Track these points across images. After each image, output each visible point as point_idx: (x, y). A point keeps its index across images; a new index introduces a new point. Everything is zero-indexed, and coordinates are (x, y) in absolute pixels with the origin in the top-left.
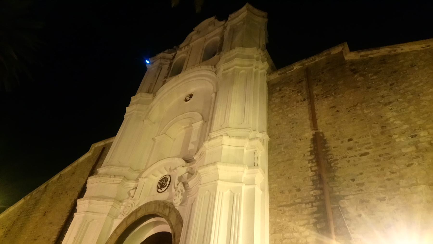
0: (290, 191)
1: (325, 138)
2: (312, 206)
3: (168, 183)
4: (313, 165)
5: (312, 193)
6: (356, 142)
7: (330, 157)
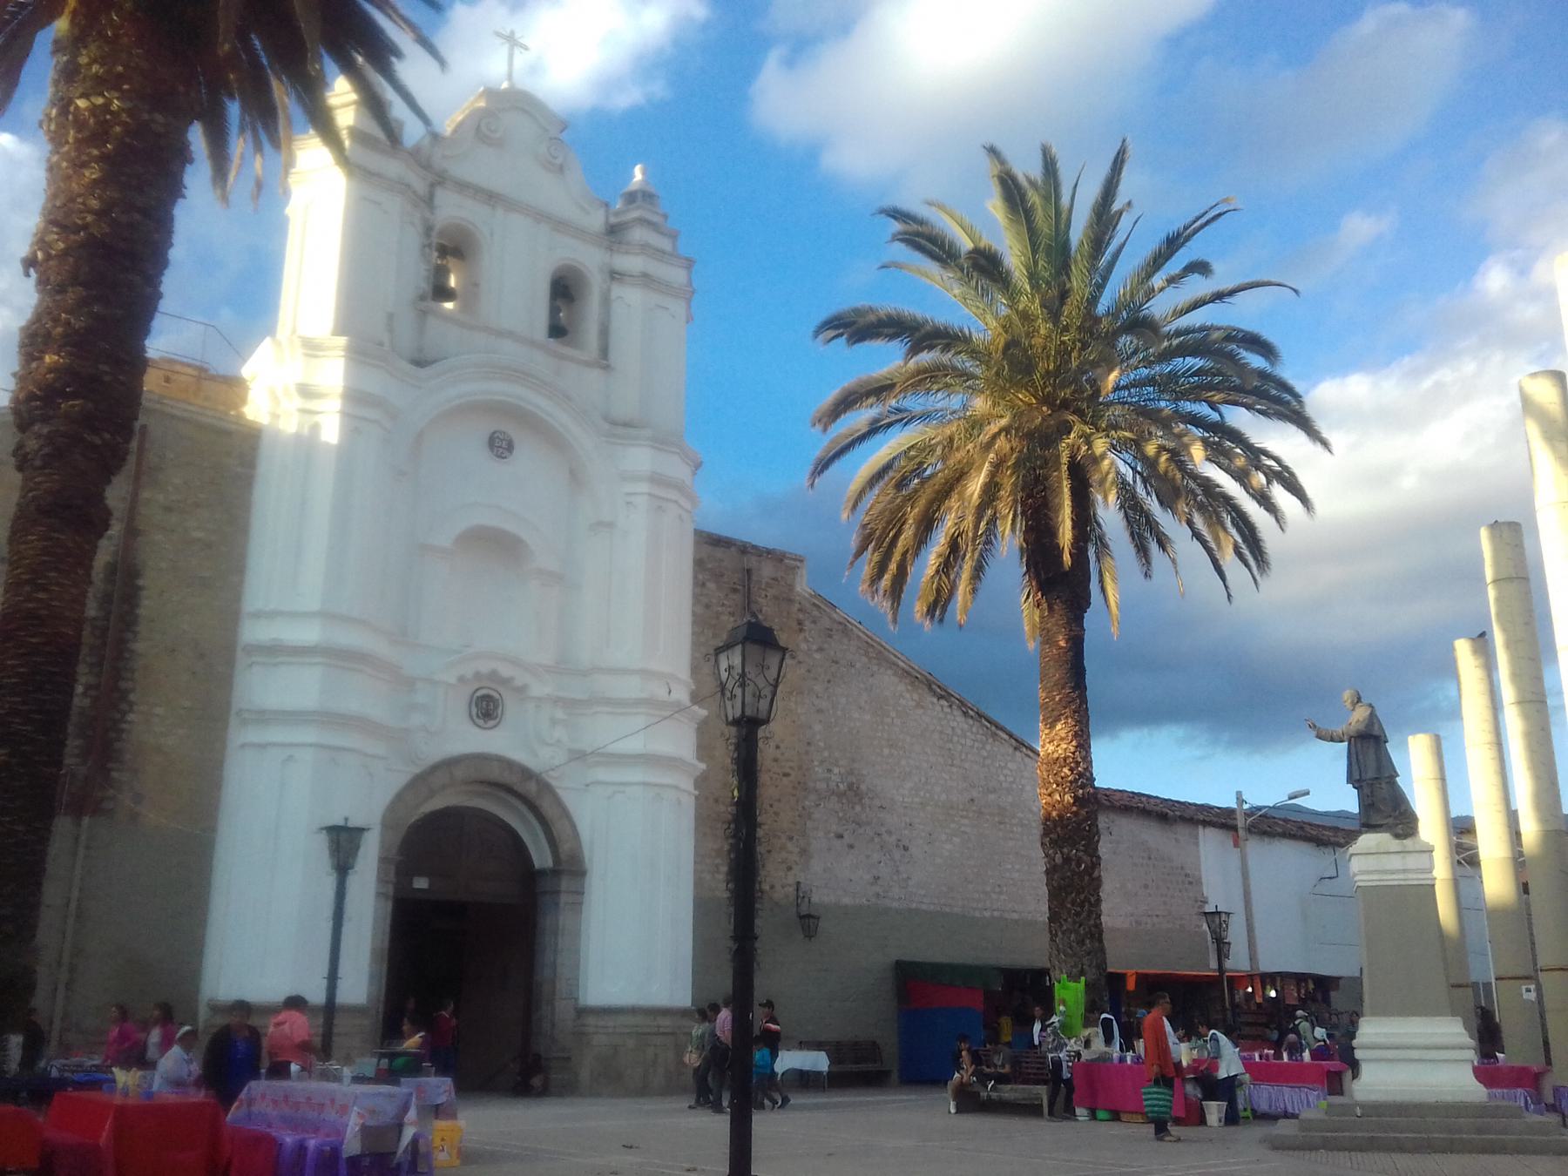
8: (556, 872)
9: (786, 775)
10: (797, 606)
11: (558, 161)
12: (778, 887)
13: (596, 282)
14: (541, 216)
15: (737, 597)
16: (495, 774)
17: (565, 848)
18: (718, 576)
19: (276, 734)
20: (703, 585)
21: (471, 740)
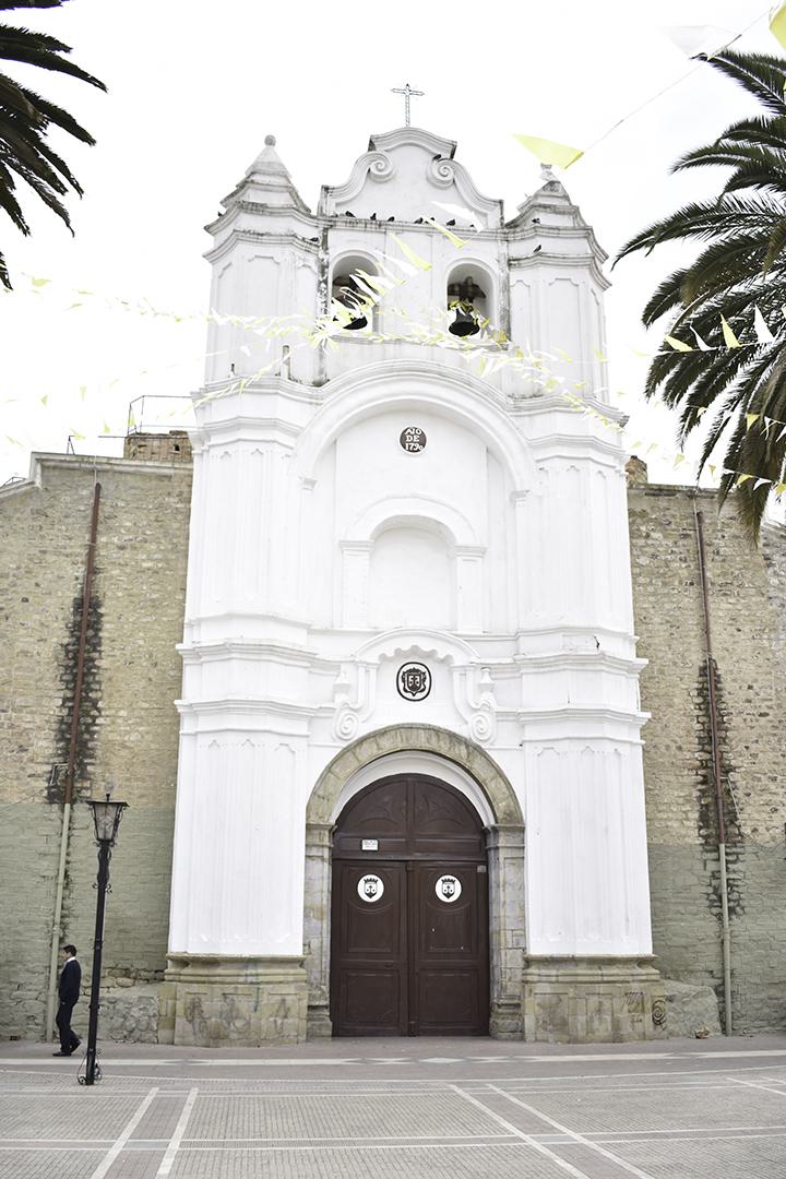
0: (668, 747)
2: (697, 774)
3: (427, 683)
4: (701, 713)
5: (696, 755)
6: (757, 694)
7: (723, 706)
8: (495, 830)
9: (768, 715)
10: (762, 541)
11: (449, 178)
12: (761, 829)
15: (691, 543)
16: (422, 740)
17: (501, 806)
18: (663, 525)
19: (205, 724)
20: (648, 536)
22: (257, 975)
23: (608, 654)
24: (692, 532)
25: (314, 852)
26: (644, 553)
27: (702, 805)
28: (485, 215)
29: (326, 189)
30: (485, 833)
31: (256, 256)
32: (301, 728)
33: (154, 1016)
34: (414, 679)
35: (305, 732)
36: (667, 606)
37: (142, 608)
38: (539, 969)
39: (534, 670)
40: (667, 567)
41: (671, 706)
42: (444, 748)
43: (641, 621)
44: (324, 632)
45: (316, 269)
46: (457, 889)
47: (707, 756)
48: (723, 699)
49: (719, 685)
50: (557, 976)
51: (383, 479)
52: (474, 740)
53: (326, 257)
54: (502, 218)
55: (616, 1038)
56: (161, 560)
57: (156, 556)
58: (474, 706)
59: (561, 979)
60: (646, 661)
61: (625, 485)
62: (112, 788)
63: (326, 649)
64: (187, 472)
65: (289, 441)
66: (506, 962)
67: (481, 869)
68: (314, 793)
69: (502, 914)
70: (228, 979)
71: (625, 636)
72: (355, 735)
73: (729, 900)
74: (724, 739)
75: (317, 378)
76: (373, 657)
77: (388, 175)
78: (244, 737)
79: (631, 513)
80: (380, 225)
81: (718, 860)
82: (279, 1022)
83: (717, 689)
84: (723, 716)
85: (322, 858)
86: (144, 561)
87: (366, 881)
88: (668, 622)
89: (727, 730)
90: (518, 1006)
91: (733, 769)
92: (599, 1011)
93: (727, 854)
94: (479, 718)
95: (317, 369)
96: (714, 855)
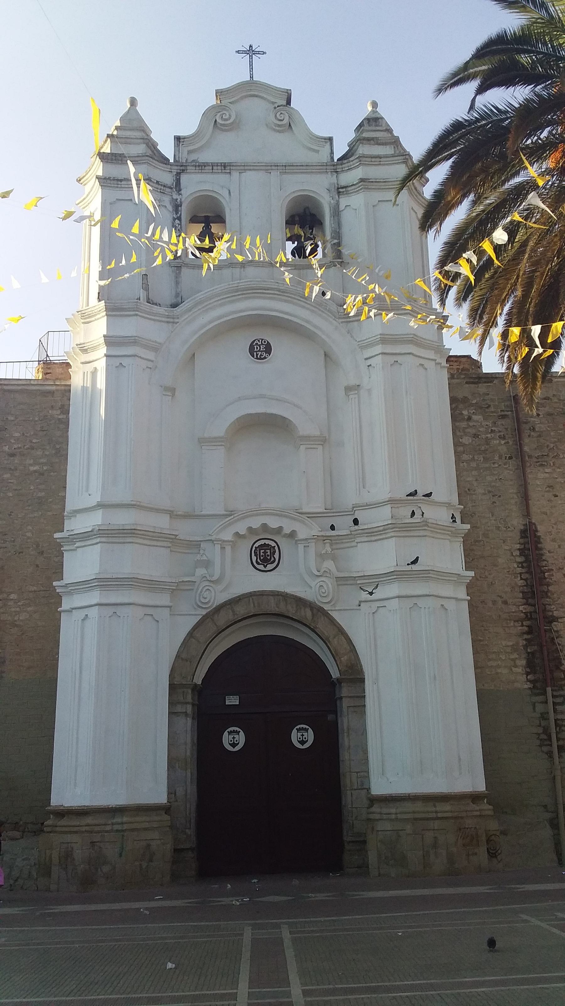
0: (494, 602)
1: (539, 534)
3: (277, 556)
4: (524, 570)
5: (521, 608)
7: (544, 563)
11: (286, 121)
13: (326, 202)
14: (269, 167)
16: (272, 606)
18: (482, 408)
20: (469, 419)
21: (250, 581)
22: (122, 823)
23: (430, 521)
24: (510, 413)
25: (179, 708)
26: (466, 434)
27: (528, 653)
28: (318, 151)
29: (178, 139)
30: (333, 685)
31: (117, 199)
32: (164, 599)
33: (35, 864)
34: (265, 553)
35: (168, 603)
36: (489, 478)
37: (29, 506)
38: (381, 808)
39: (366, 539)
40: (488, 444)
41: (495, 565)
42: (291, 610)
43: (464, 492)
44: (187, 516)
45: (170, 208)
46: (310, 736)
47: (529, 609)
48: (544, 558)
49: (539, 545)
50: (396, 814)
51: (236, 383)
52: (317, 602)
53: (179, 198)
54: (332, 153)
55: (453, 875)
56: (45, 464)
57: (43, 460)
58: (318, 574)
59: (399, 816)
60: (468, 526)
61: (445, 375)
62: (5, 662)
63: (186, 530)
64: (67, 388)
65: (150, 355)
66: (352, 800)
67: (330, 717)
68: (178, 656)
69: (347, 757)
70: (97, 829)
71: (448, 505)
72: (214, 603)
73: (558, 739)
74: (546, 593)
75: (174, 301)
76: (228, 536)
77: (232, 123)
78: (111, 610)
79: (453, 400)
80: (225, 167)
81: (546, 702)
82: (144, 865)
83: (537, 548)
84: (544, 573)
85: (186, 714)
86: (31, 465)
87: (230, 733)
88: (489, 492)
89: (548, 585)
90: (365, 842)
91: (555, 619)
92: (435, 845)
93: (553, 696)
94: (322, 583)
95: (174, 293)
96: (541, 698)
